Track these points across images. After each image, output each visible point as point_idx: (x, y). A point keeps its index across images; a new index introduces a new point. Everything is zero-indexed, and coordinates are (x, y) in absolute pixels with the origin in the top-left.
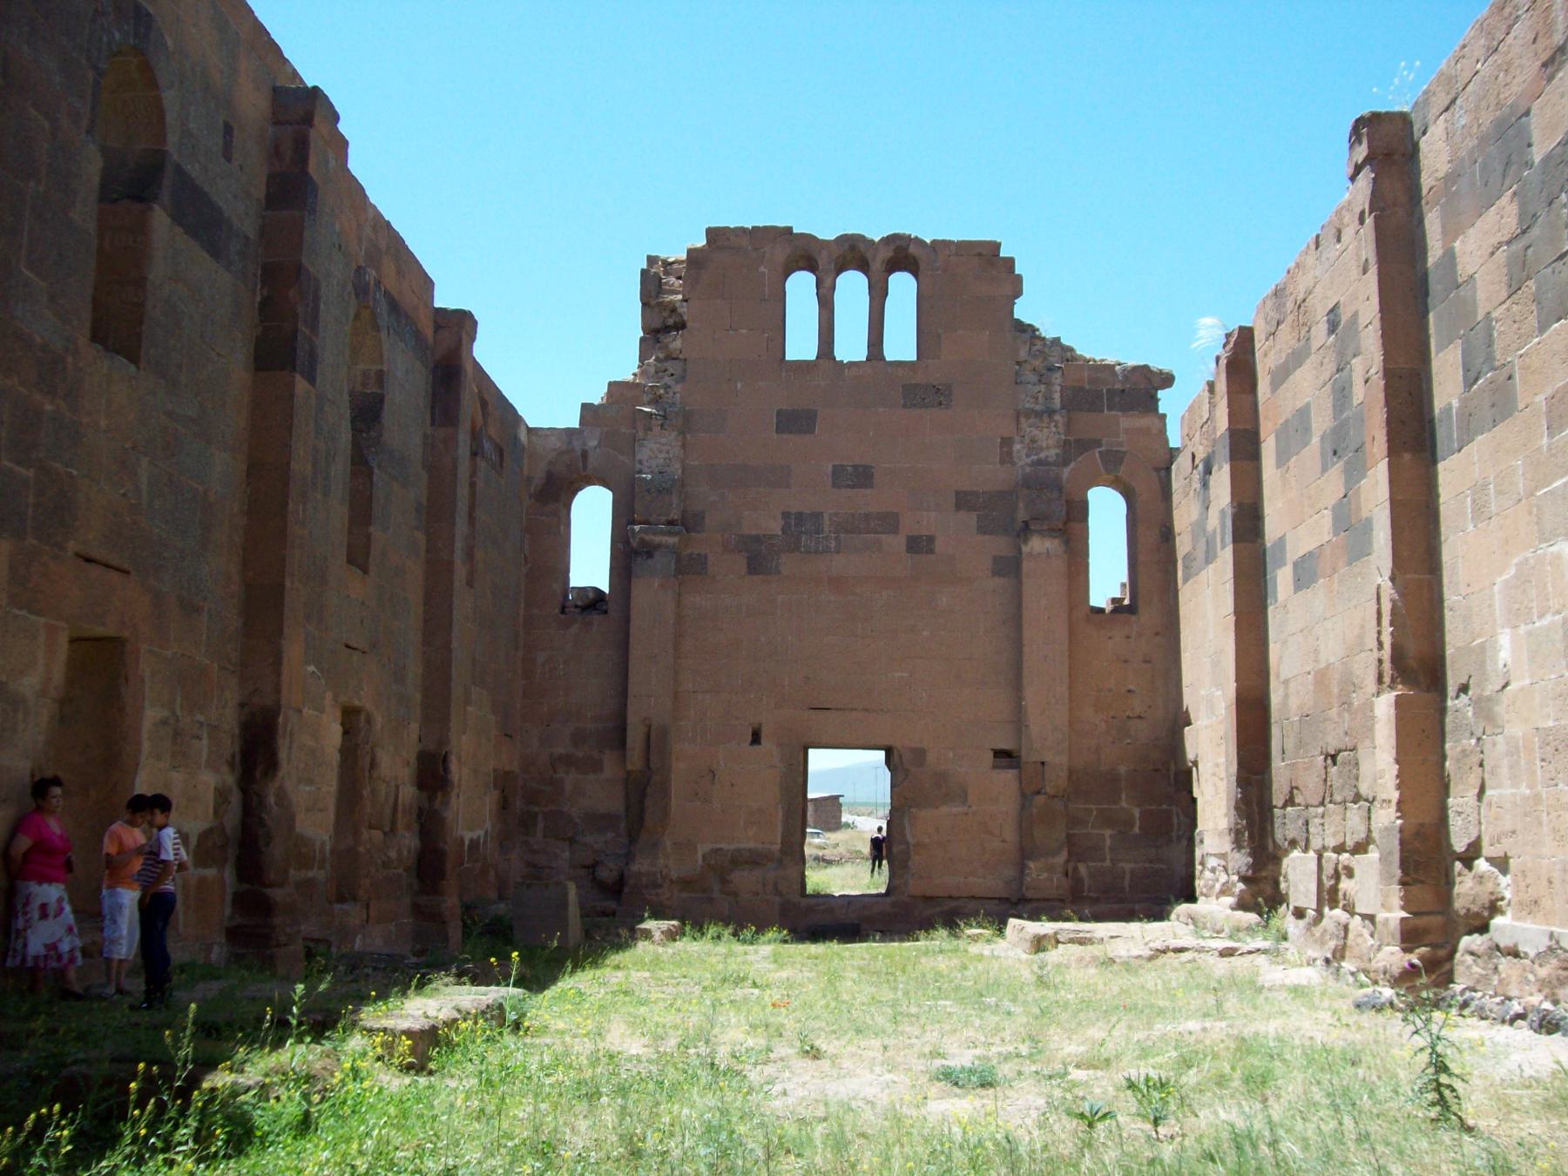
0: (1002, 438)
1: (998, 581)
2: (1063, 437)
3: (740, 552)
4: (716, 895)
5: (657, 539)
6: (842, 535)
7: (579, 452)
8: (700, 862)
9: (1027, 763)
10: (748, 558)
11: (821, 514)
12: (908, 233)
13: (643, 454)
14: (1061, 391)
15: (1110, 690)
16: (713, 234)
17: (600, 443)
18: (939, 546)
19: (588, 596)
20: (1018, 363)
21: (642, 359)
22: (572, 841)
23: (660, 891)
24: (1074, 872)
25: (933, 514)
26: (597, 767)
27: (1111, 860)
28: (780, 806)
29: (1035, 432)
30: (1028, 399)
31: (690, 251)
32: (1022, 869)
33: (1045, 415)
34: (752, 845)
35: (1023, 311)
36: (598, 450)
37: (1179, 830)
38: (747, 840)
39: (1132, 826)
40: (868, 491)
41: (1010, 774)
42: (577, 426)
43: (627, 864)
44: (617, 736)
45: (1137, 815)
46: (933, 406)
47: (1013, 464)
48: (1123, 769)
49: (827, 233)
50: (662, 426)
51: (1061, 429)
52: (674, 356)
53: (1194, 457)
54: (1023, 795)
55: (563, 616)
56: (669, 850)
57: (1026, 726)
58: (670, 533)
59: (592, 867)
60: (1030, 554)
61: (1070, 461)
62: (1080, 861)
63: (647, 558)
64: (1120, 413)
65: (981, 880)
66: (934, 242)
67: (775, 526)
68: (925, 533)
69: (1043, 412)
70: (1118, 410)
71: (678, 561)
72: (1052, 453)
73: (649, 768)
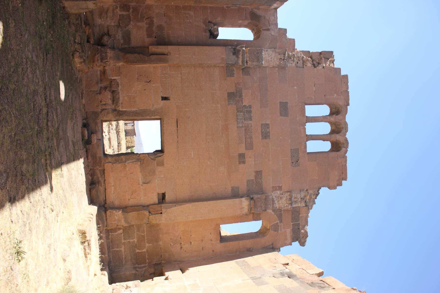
0: (281, 186)
1: (230, 190)
2: (283, 209)
3: (236, 89)
4: (100, 85)
5: (240, 56)
6: (244, 128)
7: (269, 28)
8: (113, 78)
11: (251, 120)
12: (349, 147)
13: (270, 51)
14: (298, 207)
15: (191, 236)
16: (346, 77)
17: (272, 35)
18: (242, 166)
19: (215, 32)
20: (307, 190)
21: (302, 51)
22: (119, 26)
23: (99, 61)
24: (119, 228)
25: (253, 162)
26: (149, 36)
27: (125, 243)
29: (284, 199)
30: (296, 195)
31: (339, 69)
33: (290, 202)
34: (121, 99)
35: (324, 191)
36: (270, 35)
37: (139, 268)
38: (122, 97)
39: (140, 249)
40: (261, 137)
41: (156, 200)
42: (279, 27)
43: (110, 48)
44: (162, 42)
45: (143, 251)
46: (292, 160)
47: (272, 192)
48: (161, 243)
49: (350, 118)
50: (281, 59)
51: (285, 208)
52: (304, 64)
53: (287, 264)
54: (148, 206)
55: (207, 21)
56: (117, 65)
57: (176, 205)
58: (243, 62)
59: (108, 34)
60: (241, 201)
61: (274, 212)
62: (123, 230)
63: (233, 53)
64: (291, 229)
65: (113, 192)
66: (346, 157)
67: (246, 103)
68: (246, 160)
70: (292, 228)
71: (233, 65)
72: (277, 205)
73: (150, 55)
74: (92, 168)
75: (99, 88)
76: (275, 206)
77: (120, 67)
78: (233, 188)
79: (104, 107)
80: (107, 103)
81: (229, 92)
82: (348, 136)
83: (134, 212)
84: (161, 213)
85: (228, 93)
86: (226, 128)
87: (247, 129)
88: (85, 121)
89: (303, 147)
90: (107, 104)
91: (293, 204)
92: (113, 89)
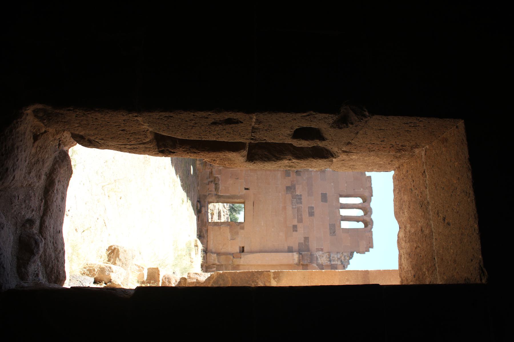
1: (287, 248)
4: (208, 180)
6: (296, 209)
8: (216, 176)
9: (241, 254)
10: (290, 187)
14: (336, 264)
18: (295, 233)
20: (342, 253)
23: (209, 166)
24: (214, 267)
25: (303, 231)
28: (230, 195)
29: (325, 257)
32: (215, 253)
34: (220, 188)
38: (221, 187)
41: (238, 251)
46: (330, 231)
47: (316, 252)
49: (373, 205)
51: (326, 264)
54: (233, 254)
62: (216, 268)
65: (212, 243)
66: (372, 232)
68: (298, 229)
69: (330, 259)
72: (320, 261)
74: (200, 228)
75: (208, 182)
76: (319, 262)
77: (220, 170)
78: (289, 247)
79: (210, 193)
80: (212, 190)
81: (287, 186)
82: (373, 217)
83: (224, 256)
84: (241, 258)
85: (286, 187)
86: (284, 208)
87: (299, 210)
88: (198, 200)
89: (338, 223)
90: (212, 191)
91: (332, 261)
92: (216, 182)
